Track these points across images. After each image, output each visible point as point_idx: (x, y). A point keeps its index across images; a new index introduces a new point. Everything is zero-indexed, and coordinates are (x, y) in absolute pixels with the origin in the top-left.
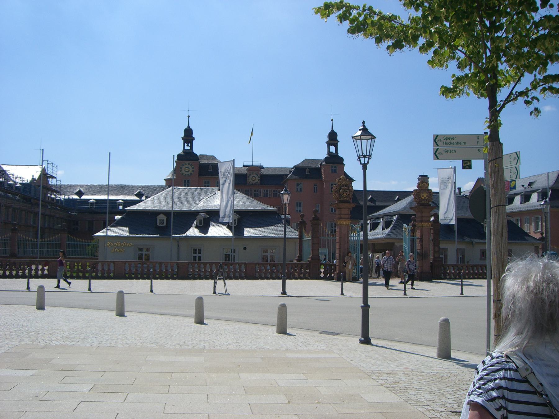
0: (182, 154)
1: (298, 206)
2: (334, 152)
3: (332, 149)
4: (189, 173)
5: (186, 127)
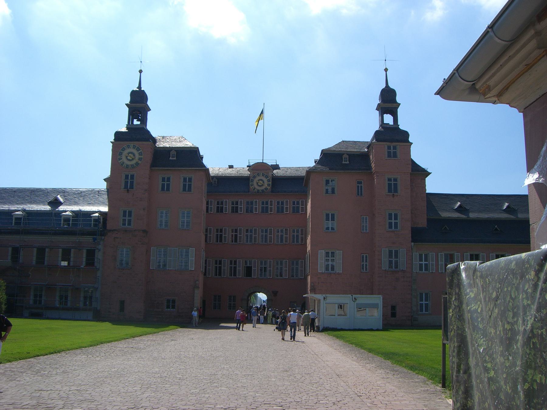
1: (327, 219)
2: (391, 123)
3: (388, 119)
4: (133, 162)
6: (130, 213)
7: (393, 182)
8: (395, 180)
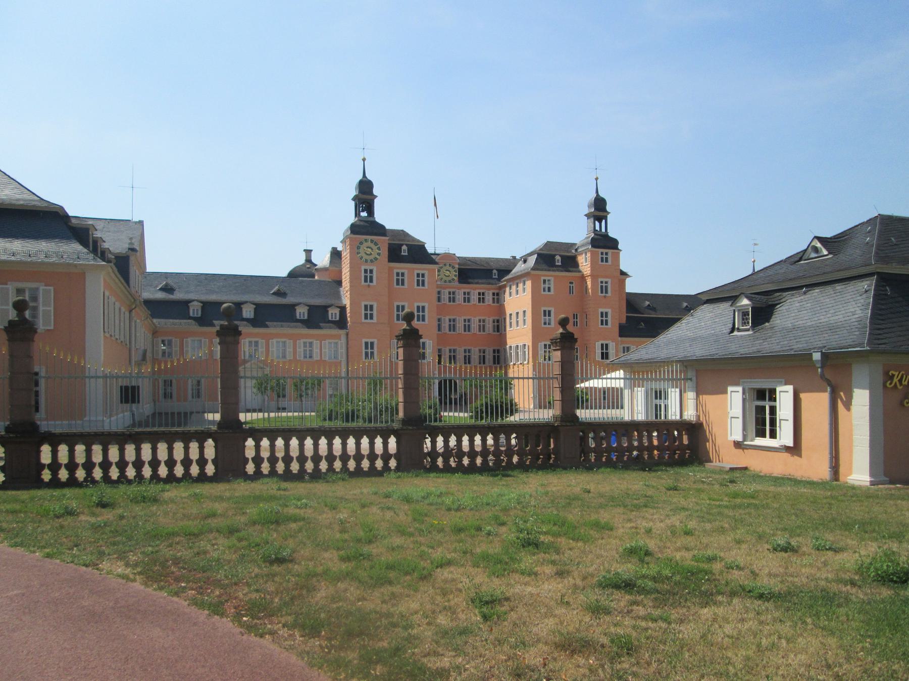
0: (358, 224)
1: (545, 315)
4: (372, 257)
5: (360, 177)
6: (371, 307)
7: (604, 285)
8: (606, 283)
